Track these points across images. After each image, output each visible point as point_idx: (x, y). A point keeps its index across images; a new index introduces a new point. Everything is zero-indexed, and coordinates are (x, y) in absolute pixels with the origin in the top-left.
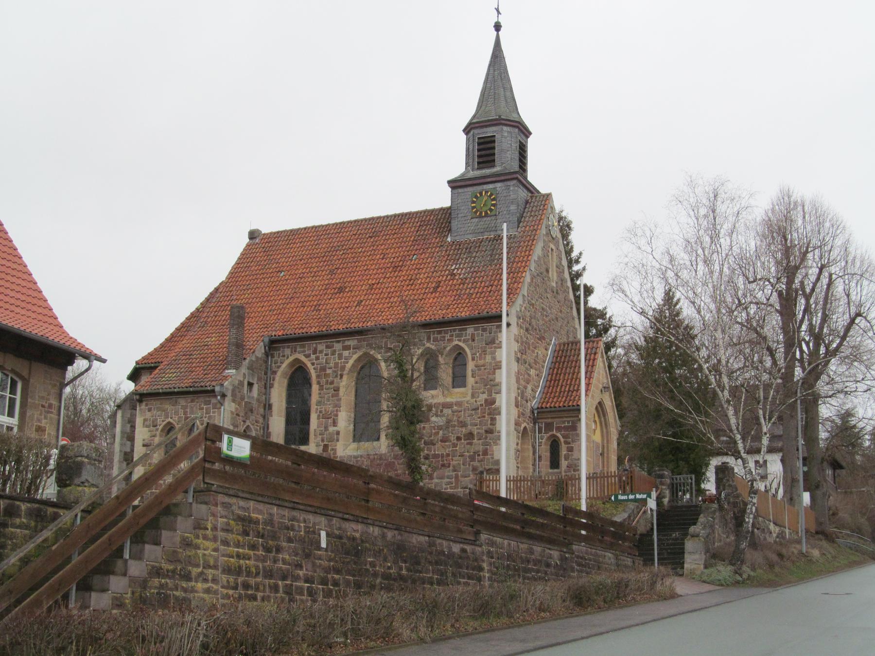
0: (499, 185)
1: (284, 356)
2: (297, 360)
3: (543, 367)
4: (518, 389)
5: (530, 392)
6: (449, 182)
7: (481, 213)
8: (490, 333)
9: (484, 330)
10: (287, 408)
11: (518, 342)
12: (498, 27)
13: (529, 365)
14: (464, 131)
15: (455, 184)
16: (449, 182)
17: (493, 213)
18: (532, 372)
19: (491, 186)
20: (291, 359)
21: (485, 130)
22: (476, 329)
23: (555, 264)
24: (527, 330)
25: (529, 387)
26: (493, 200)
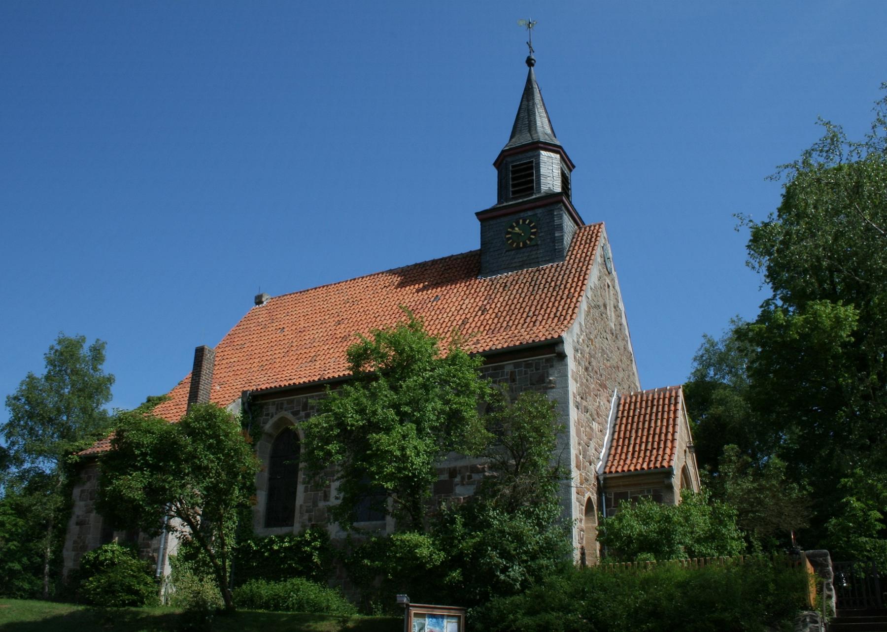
0: (539, 211)
1: (267, 415)
2: (283, 420)
3: (607, 422)
4: (579, 444)
5: (594, 451)
6: (477, 214)
7: (518, 244)
8: (537, 369)
9: (528, 365)
10: (270, 479)
11: (577, 382)
12: (530, 62)
13: (591, 415)
14: (495, 164)
15: (484, 217)
16: (477, 214)
17: (533, 243)
18: (595, 426)
19: (530, 213)
20: (275, 419)
21: (520, 156)
22: (516, 365)
23: (612, 303)
24: (586, 369)
25: (593, 444)
26: (533, 228)
